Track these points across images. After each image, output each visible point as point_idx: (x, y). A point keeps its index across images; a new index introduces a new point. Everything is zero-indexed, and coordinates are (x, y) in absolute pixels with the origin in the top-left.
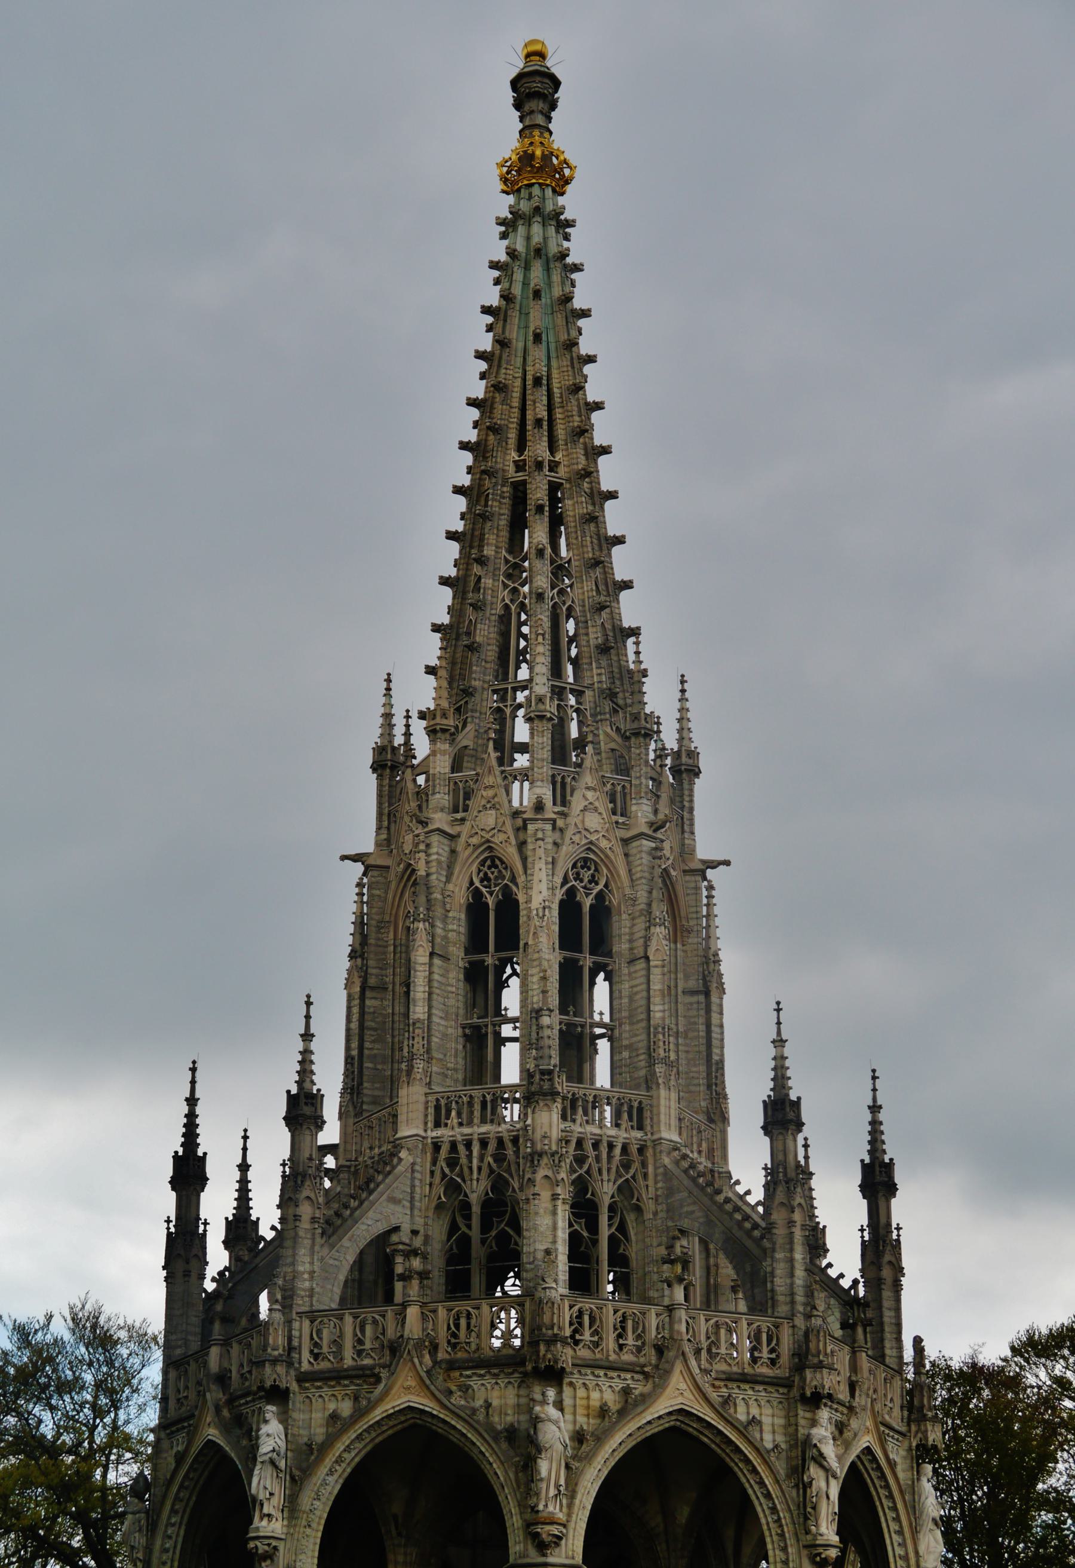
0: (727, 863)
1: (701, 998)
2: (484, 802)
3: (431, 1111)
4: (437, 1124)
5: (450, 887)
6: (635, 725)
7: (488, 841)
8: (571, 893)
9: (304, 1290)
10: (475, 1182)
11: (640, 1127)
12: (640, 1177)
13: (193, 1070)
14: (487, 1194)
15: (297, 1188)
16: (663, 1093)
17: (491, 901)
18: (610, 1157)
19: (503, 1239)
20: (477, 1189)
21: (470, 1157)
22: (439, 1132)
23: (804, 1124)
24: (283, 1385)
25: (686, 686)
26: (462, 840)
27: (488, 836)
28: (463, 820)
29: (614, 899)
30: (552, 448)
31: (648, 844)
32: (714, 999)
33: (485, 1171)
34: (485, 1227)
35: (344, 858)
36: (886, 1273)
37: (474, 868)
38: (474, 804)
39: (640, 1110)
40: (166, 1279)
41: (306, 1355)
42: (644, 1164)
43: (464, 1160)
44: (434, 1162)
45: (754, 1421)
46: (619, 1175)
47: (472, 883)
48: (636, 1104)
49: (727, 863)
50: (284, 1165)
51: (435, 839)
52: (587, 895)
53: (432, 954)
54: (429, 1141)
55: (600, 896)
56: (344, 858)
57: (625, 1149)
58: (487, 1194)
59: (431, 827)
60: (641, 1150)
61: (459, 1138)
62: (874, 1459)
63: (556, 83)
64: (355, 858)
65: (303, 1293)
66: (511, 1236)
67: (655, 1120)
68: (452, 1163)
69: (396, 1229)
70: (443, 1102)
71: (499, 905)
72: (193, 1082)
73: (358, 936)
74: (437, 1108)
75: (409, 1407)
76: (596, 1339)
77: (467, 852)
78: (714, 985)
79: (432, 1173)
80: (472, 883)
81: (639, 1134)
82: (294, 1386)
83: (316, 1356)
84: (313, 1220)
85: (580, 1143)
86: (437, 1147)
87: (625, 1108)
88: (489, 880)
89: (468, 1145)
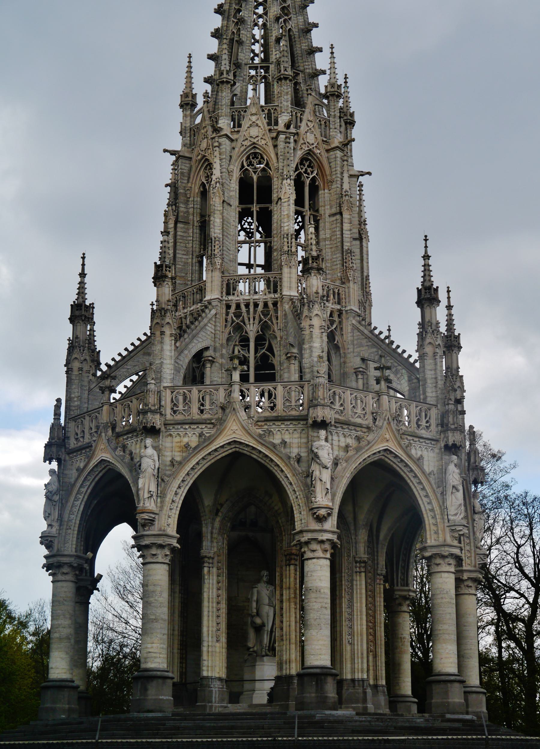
0: (369, 173)
1: (358, 242)
2: (251, 123)
3: (225, 286)
4: (228, 294)
5: (231, 167)
6: (333, 90)
7: (254, 143)
8: (299, 175)
9: (75, 407)
10: (252, 325)
11: (339, 303)
12: (338, 329)
13: (83, 258)
14: (258, 332)
15: (163, 317)
17: (255, 177)
19: (265, 358)
20: (252, 330)
21: (248, 312)
22: (230, 298)
23: (440, 301)
24: (158, 427)
25: (348, 80)
26: (240, 141)
27: (255, 141)
28: (238, 132)
29: (319, 182)
31: (339, 153)
32: (364, 244)
33: (257, 321)
34: (256, 351)
35: (165, 151)
37: (244, 158)
38: (245, 124)
39: (339, 294)
40: (67, 372)
41: (169, 411)
42: (340, 323)
43: (245, 314)
44: (227, 314)
45: (421, 458)
47: (243, 166)
48: (336, 291)
49: (369, 173)
50: (152, 304)
51: (224, 140)
52: (308, 178)
53: (224, 201)
54: (224, 302)
55: (314, 180)
56: (165, 151)
58: (258, 332)
59: (222, 133)
61: (242, 301)
64: (173, 153)
65: (73, 408)
66: (268, 356)
67: (347, 300)
68: (238, 315)
69: (207, 349)
70: (231, 282)
71: (258, 178)
72: (83, 265)
73: (173, 194)
74: (228, 285)
75: (235, 441)
76: (342, 408)
77: (242, 149)
78: (364, 236)
79: (226, 321)
80: (243, 166)
81: (339, 307)
82: (163, 429)
83: (175, 412)
84: (171, 335)
86: (228, 307)
87: (331, 292)
88: (253, 165)
89: (247, 306)
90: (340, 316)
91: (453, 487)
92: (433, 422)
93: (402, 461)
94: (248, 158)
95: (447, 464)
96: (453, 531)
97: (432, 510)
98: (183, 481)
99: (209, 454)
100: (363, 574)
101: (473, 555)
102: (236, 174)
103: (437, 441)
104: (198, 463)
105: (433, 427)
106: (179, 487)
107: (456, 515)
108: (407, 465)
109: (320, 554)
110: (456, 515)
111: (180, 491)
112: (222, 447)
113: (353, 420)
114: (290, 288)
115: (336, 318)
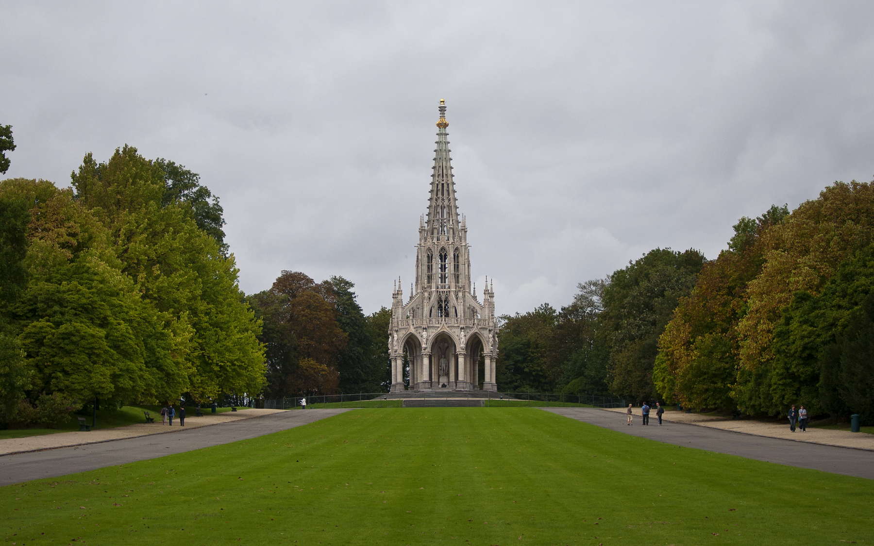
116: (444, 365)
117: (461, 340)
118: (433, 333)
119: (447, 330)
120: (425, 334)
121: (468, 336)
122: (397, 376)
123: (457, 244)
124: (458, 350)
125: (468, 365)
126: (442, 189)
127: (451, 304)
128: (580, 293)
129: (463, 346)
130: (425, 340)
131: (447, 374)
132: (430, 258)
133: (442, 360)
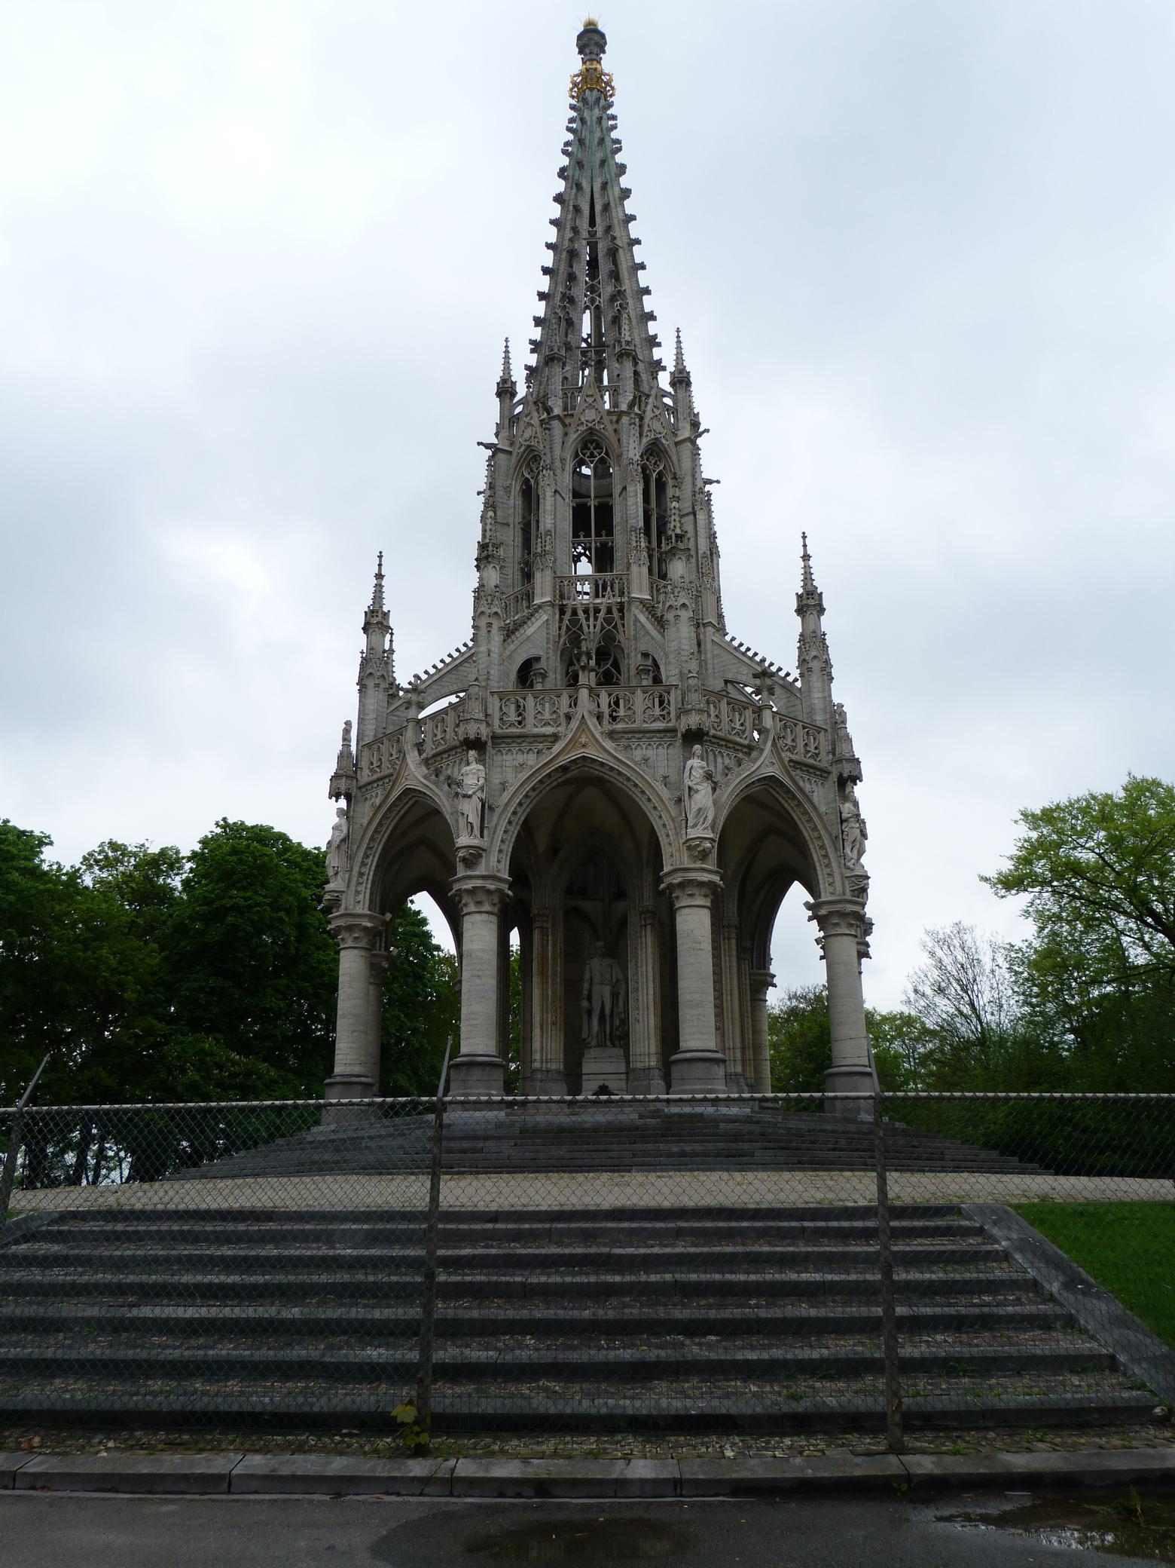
1: (691, 517)
12: (619, 626)
16: (634, 568)
18: (596, 619)
30: (592, 222)
36: (816, 665)
42: (622, 618)
46: (603, 628)
57: (609, 611)
60: (621, 610)
62: (781, 784)
63: (603, 36)
85: (574, 613)
90: (621, 610)
91: (690, 788)
92: (672, 708)
93: (612, 769)
94: (528, 465)
95: (686, 759)
96: (689, 848)
97: (664, 826)
98: (369, 848)
99: (389, 810)
100: (649, 928)
101: (838, 879)
102: (516, 488)
103: (674, 731)
104: (380, 824)
105: (673, 715)
106: (366, 856)
107: (695, 825)
108: (620, 773)
109: (472, 908)
110: (695, 825)
111: (369, 861)
112: (399, 798)
113: (536, 731)
114: (542, 595)
115: (616, 614)
116: (603, 993)
117: (690, 805)
118: (515, 773)
119: (603, 750)
120: (472, 773)
121: (730, 791)
122: (351, 1050)
123: (655, 427)
124: (674, 858)
125: (732, 982)
126: (593, 254)
127: (633, 661)
128: (1034, 835)
129: (702, 831)
130: (470, 809)
131: (619, 1037)
132: (530, 496)
133: (597, 967)
